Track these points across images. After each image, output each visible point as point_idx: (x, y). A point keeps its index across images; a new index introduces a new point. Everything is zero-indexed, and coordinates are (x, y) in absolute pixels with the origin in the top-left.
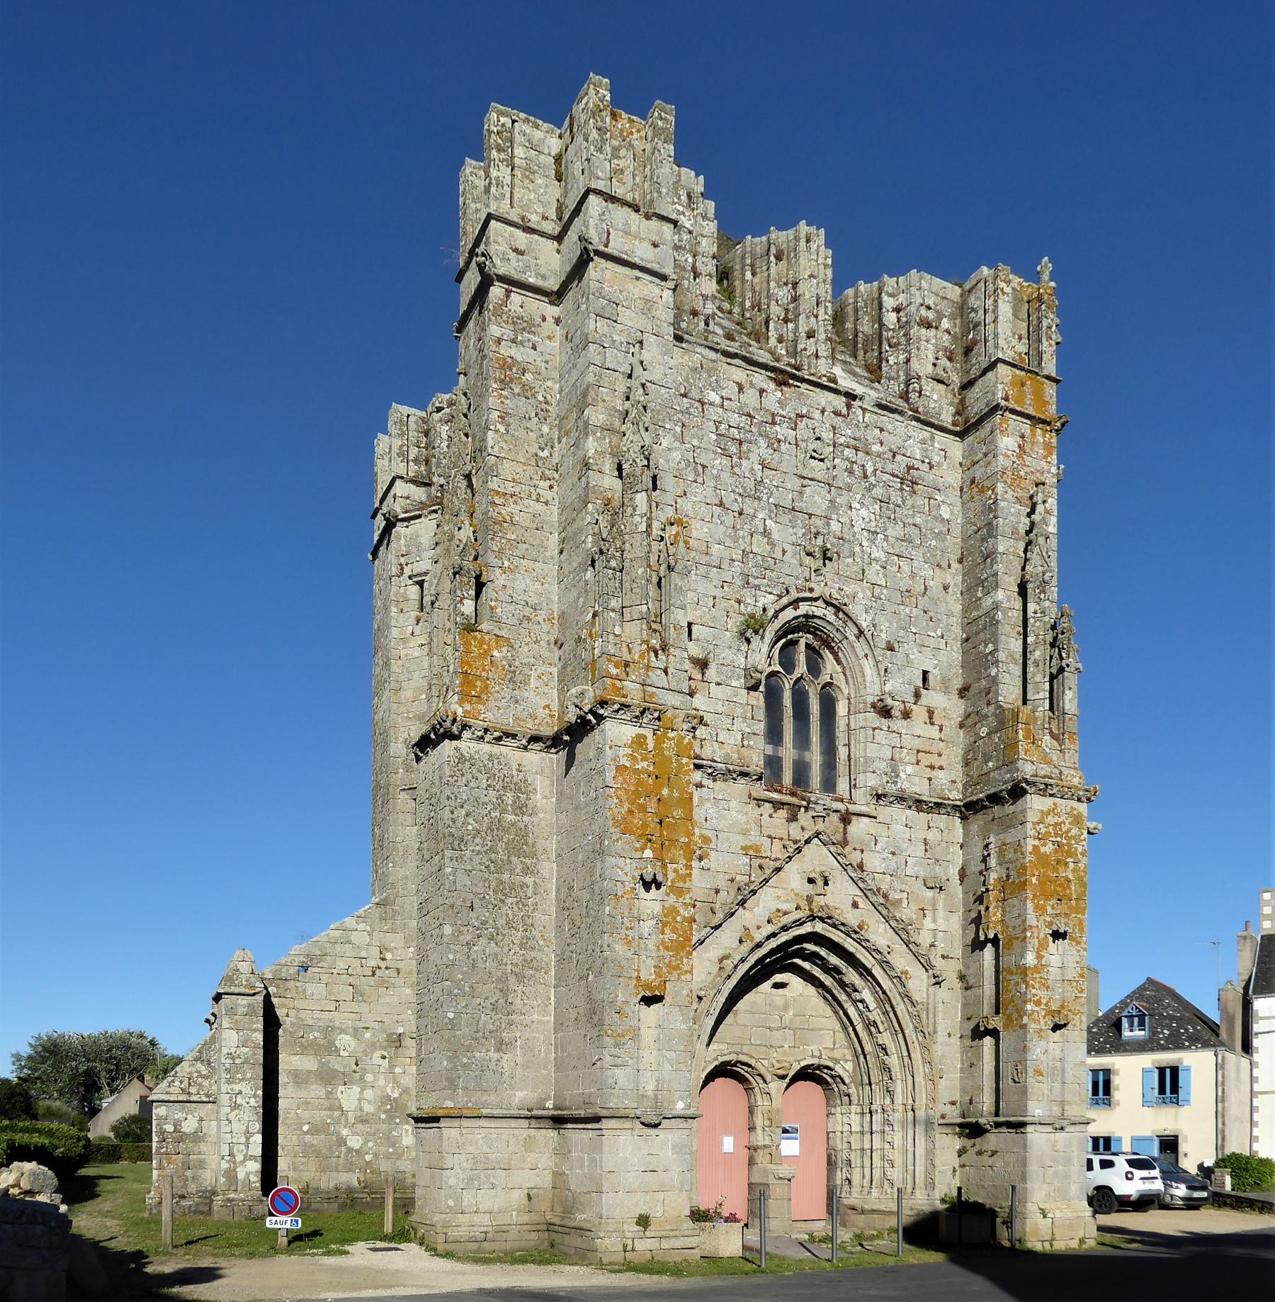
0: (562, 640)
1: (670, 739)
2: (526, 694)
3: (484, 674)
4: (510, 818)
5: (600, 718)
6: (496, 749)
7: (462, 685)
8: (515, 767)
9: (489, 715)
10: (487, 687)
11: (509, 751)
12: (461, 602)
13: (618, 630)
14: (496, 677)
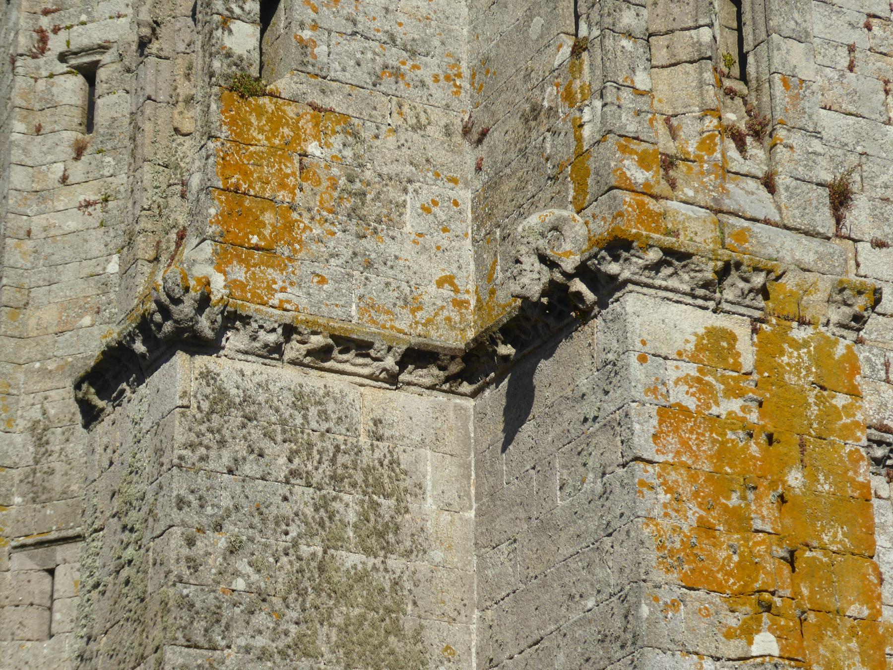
0: (484, 120)
1: (797, 345)
2: (393, 249)
3: (282, 195)
4: (351, 559)
5: (608, 287)
6: (314, 381)
7: (226, 217)
8: (364, 425)
9: (296, 297)
10: (290, 226)
11: (349, 389)
12: (225, 24)
13: (642, 80)
14: (315, 204)
